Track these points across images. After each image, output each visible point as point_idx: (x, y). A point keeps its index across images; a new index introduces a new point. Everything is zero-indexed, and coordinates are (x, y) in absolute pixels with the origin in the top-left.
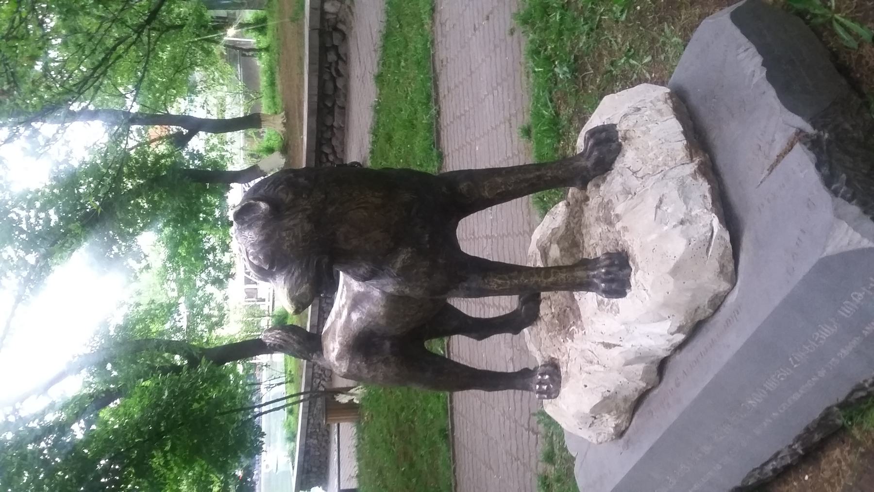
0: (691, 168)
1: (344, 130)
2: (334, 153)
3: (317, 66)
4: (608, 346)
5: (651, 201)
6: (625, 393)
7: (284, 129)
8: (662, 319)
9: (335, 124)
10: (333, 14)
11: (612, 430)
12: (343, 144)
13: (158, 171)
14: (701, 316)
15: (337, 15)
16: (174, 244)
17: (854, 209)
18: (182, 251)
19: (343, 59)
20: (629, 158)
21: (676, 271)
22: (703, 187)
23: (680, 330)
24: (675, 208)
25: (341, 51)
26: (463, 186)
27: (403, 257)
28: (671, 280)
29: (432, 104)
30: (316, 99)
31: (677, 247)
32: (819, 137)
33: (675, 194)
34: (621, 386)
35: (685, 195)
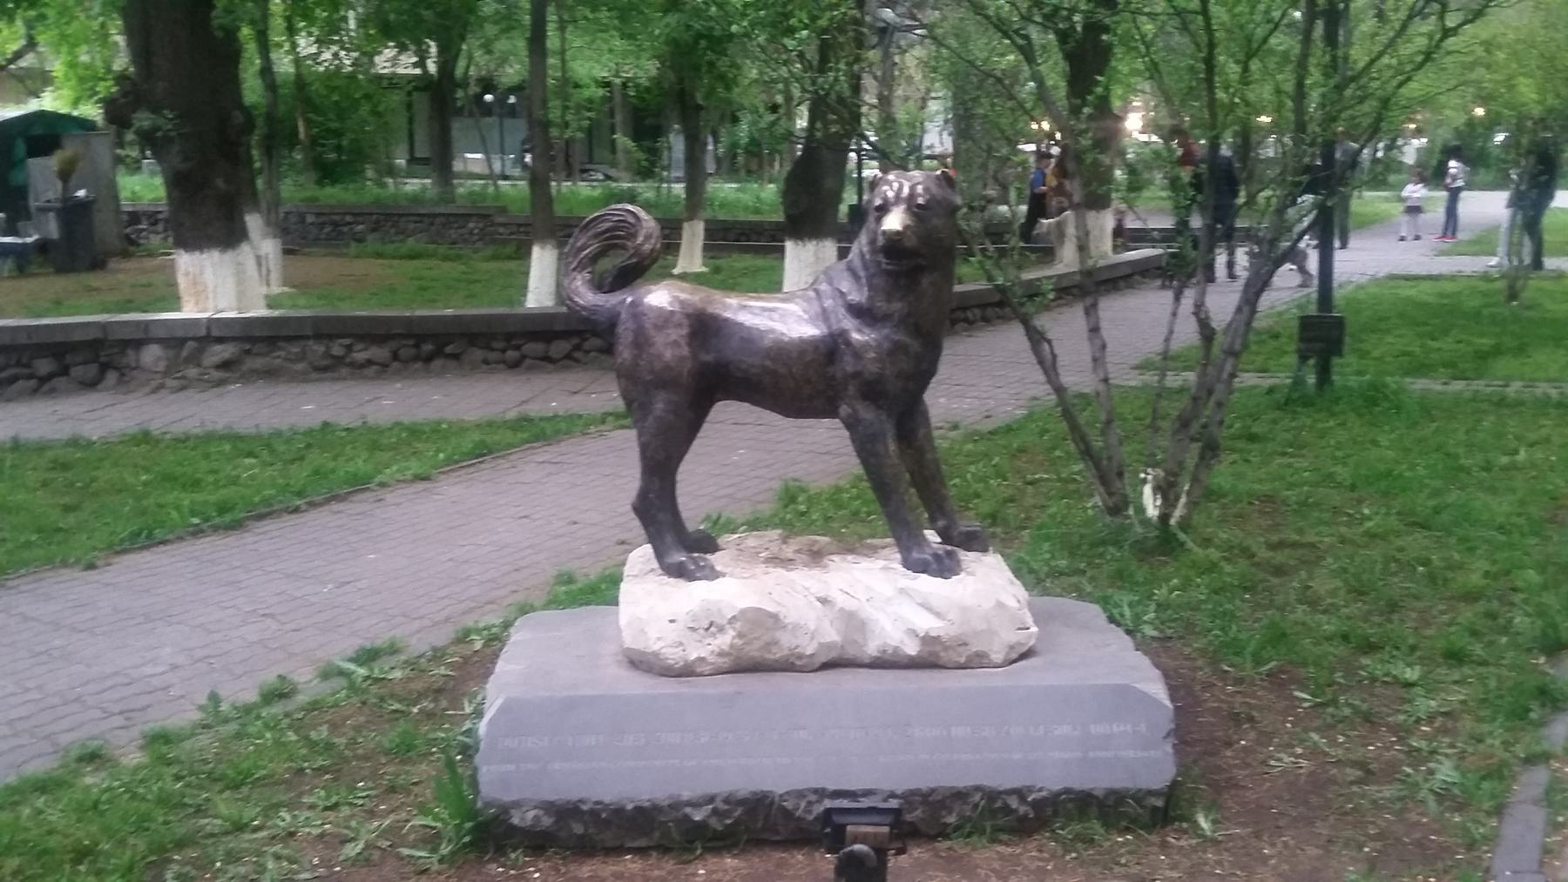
10: (138, 360)
11: (693, 656)
14: (945, 657)
19: (42, 386)
23: (928, 640)
25: (60, 382)
28: (993, 603)
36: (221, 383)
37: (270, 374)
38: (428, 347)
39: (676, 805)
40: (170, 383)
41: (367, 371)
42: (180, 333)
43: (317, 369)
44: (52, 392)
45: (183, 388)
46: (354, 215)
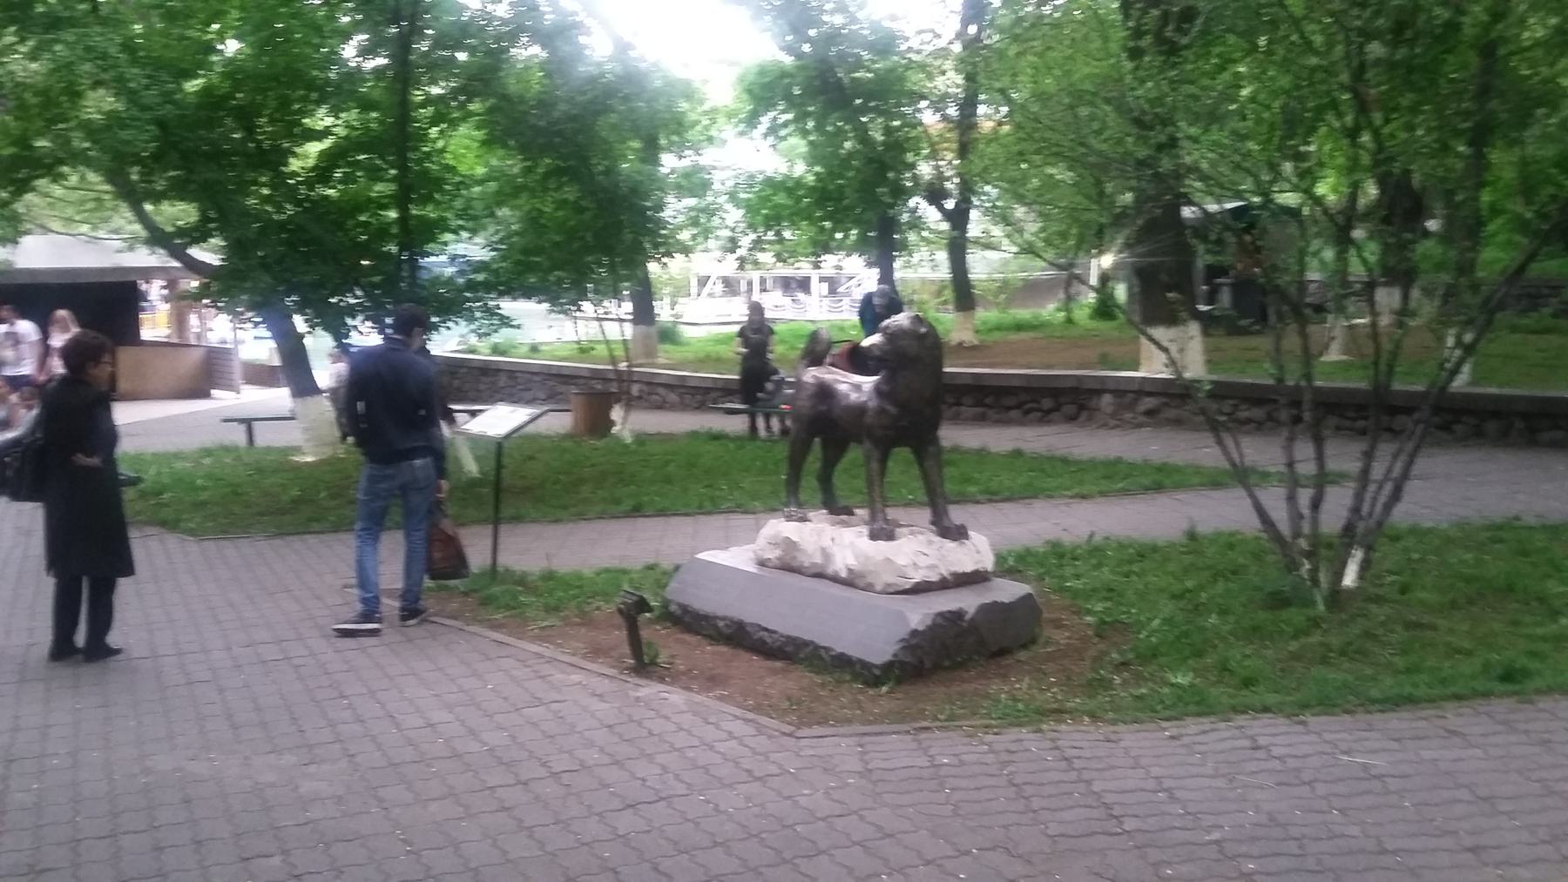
0: (945, 574)
3: (1035, 385)
6: (798, 554)
7: (953, 343)
8: (857, 557)
9: (963, 408)
15: (1098, 410)
16: (789, 187)
17: (929, 622)
18: (781, 199)
19: (1045, 417)
21: (888, 560)
22: (934, 578)
23: (850, 571)
25: (1055, 415)
26: (931, 449)
27: (892, 409)
29: (988, 496)
31: (901, 561)
32: (962, 620)
34: (803, 551)
35: (932, 567)
36: (1140, 426)
37: (1178, 423)
39: (716, 618)
40: (1113, 422)
41: (1247, 427)
44: (1049, 422)
45: (1117, 426)
46: (1548, 287)
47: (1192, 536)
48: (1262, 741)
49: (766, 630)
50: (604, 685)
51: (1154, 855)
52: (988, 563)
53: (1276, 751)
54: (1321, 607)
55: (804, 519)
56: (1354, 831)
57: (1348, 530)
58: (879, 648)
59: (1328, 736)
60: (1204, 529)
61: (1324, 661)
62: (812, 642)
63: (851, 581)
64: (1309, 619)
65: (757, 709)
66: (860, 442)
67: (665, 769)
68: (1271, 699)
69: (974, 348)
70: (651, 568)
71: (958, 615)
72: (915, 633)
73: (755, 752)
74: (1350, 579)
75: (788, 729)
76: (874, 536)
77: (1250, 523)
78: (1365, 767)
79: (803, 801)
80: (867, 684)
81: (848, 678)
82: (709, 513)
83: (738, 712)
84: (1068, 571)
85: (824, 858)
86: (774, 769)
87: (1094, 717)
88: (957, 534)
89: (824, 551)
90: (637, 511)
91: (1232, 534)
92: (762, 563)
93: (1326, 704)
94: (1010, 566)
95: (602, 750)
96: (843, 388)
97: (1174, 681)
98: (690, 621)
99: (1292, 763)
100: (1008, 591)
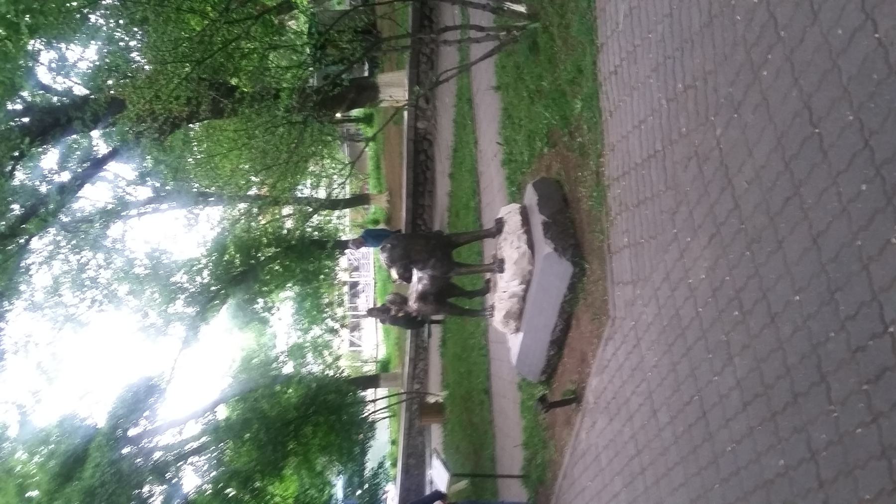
0: (522, 231)
1: (431, 207)
2: (425, 224)
4: (505, 292)
5: (510, 241)
7: (387, 205)
12: (431, 217)
13: (290, 241)
14: (527, 278)
16: (301, 299)
17: (549, 241)
18: (308, 304)
19: (430, 158)
20: (506, 228)
21: (515, 263)
22: (525, 237)
23: (521, 283)
24: (516, 244)
25: (429, 153)
27: (432, 261)
30: (411, 186)
33: (516, 239)
34: (511, 307)
35: (519, 238)
36: (435, 107)
38: (426, 23)
40: (433, 122)
42: (413, 117)
43: (432, 68)
47: (498, 88)
48: (612, 69)
49: (555, 328)
50: (587, 422)
51: (675, 136)
52: (516, 207)
53: (617, 63)
54: (537, 25)
55: (493, 307)
56: (660, 28)
57: (494, 11)
58: (564, 269)
59: (609, 33)
60: (494, 83)
61: (567, 27)
62: (562, 303)
63: (527, 283)
64: (544, 32)
65: (599, 337)
66: (450, 278)
67: (633, 393)
68: (588, 59)
69: (390, 194)
70: (520, 388)
71: (546, 226)
72: (556, 250)
73: (622, 343)
74: (521, 8)
75: (610, 322)
76: (502, 271)
77: (491, 61)
78: (625, 16)
79: (650, 320)
80: (584, 275)
81: (580, 285)
82: (488, 351)
83: (600, 349)
84: (519, 158)
85: (681, 312)
86: (632, 333)
87: (600, 156)
88: (500, 224)
89: (510, 297)
90: (487, 392)
91: (497, 66)
92: (518, 330)
93: (591, 30)
94: (516, 195)
95: (624, 426)
96: (420, 287)
97: (579, 110)
98: (550, 371)
99: (624, 55)
100: (531, 196)
